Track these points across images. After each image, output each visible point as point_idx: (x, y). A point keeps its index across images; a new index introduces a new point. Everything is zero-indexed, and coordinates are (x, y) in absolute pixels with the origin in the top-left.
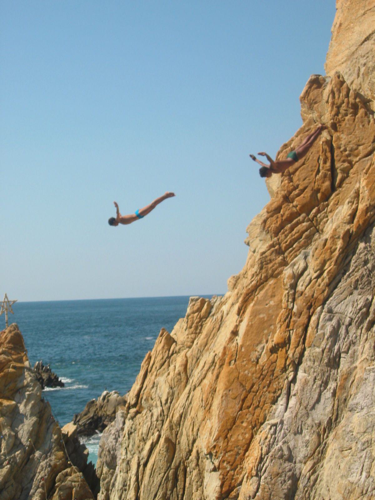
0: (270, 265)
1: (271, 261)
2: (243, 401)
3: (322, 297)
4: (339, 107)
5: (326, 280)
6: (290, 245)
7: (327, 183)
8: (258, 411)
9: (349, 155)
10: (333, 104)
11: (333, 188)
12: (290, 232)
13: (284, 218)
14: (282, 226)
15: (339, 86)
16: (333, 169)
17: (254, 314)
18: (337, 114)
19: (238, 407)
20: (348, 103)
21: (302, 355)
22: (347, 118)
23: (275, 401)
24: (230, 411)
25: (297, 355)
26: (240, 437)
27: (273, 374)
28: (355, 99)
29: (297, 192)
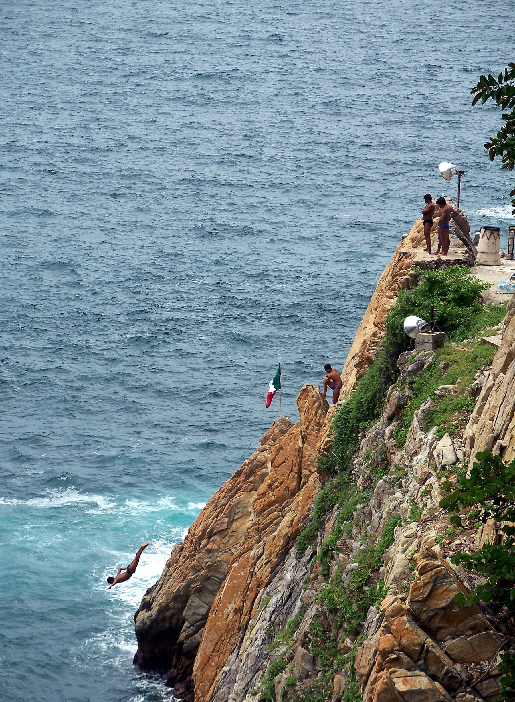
0: (251, 540)
1: (252, 537)
2: (216, 644)
3: (266, 581)
4: (310, 422)
5: (270, 569)
6: (265, 528)
7: (295, 484)
8: (221, 655)
9: (309, 465)
10: (306, 418)
11: (299, 487)
12: (267, 517)
13: (265, 503)
14: (263, 510)
15: (312, 404)
16: (299, 473)
17: (232, 579)
18: (307, 428)
19: (212, 648)
20: (315, 421)
21: (248, 622)
22: (314, 433)
23: (232, 652)
24: (207, 650)
25: (245, 623)
26: (209, 674)
27: (233, 630)
28: (320, 419)
29: (276, 484)
